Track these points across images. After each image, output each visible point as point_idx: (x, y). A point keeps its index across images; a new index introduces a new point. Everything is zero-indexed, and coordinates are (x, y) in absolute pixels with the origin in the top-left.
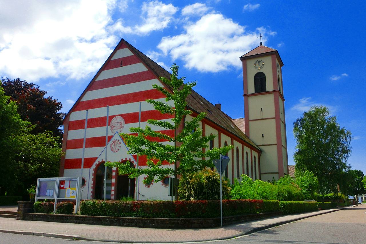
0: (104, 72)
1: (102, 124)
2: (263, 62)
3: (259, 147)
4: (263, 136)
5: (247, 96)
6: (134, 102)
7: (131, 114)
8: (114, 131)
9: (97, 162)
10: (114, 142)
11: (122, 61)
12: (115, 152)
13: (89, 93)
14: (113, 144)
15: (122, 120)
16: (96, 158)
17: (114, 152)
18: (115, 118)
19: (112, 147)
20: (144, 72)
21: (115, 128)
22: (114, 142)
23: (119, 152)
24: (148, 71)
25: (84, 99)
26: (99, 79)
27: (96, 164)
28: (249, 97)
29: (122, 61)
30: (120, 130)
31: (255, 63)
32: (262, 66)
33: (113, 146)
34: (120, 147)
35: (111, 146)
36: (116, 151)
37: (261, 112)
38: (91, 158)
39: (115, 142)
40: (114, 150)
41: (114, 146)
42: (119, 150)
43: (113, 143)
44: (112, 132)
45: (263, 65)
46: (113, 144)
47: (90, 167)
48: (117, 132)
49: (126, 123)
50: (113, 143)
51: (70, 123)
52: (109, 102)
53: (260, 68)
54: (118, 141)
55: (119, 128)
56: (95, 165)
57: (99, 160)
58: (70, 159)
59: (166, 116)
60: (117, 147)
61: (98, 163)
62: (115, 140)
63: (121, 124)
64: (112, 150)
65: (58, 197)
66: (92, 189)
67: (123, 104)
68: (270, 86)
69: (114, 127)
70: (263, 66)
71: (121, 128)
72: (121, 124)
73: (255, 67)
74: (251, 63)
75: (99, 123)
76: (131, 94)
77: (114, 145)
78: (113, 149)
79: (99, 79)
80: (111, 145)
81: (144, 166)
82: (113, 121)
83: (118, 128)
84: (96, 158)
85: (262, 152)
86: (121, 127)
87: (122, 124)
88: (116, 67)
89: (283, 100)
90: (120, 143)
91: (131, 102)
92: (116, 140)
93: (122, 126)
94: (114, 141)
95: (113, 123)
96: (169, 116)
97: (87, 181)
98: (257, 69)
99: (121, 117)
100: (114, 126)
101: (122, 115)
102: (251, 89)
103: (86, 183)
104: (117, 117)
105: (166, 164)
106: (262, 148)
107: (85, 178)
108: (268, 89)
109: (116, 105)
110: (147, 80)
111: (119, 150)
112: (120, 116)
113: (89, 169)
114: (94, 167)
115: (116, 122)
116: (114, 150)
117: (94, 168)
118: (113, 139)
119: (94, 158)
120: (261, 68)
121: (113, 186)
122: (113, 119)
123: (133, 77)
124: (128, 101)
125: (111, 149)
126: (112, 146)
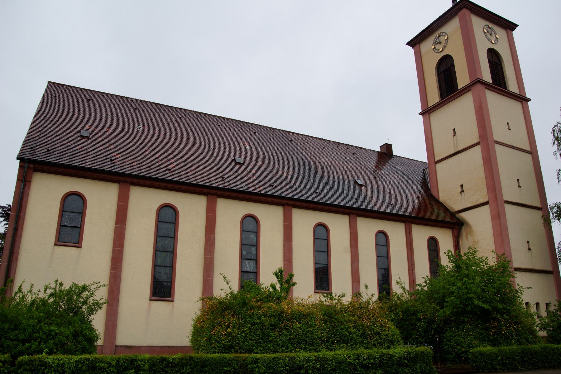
2: (446, 34)
3: (457, 215)
4: (463, 191)
5: (427, 112)
28: (431, 115)
31: (433, 43)
32: (446, 42)
53: (441, 50)
68: (462, 80)
70: (447, 42)
74: (427, 46)
85: (463, 227)
89: (523, 99)
98: (438, 53)
102: (434, 97)
106: (464, 215)
120: (444, 47)
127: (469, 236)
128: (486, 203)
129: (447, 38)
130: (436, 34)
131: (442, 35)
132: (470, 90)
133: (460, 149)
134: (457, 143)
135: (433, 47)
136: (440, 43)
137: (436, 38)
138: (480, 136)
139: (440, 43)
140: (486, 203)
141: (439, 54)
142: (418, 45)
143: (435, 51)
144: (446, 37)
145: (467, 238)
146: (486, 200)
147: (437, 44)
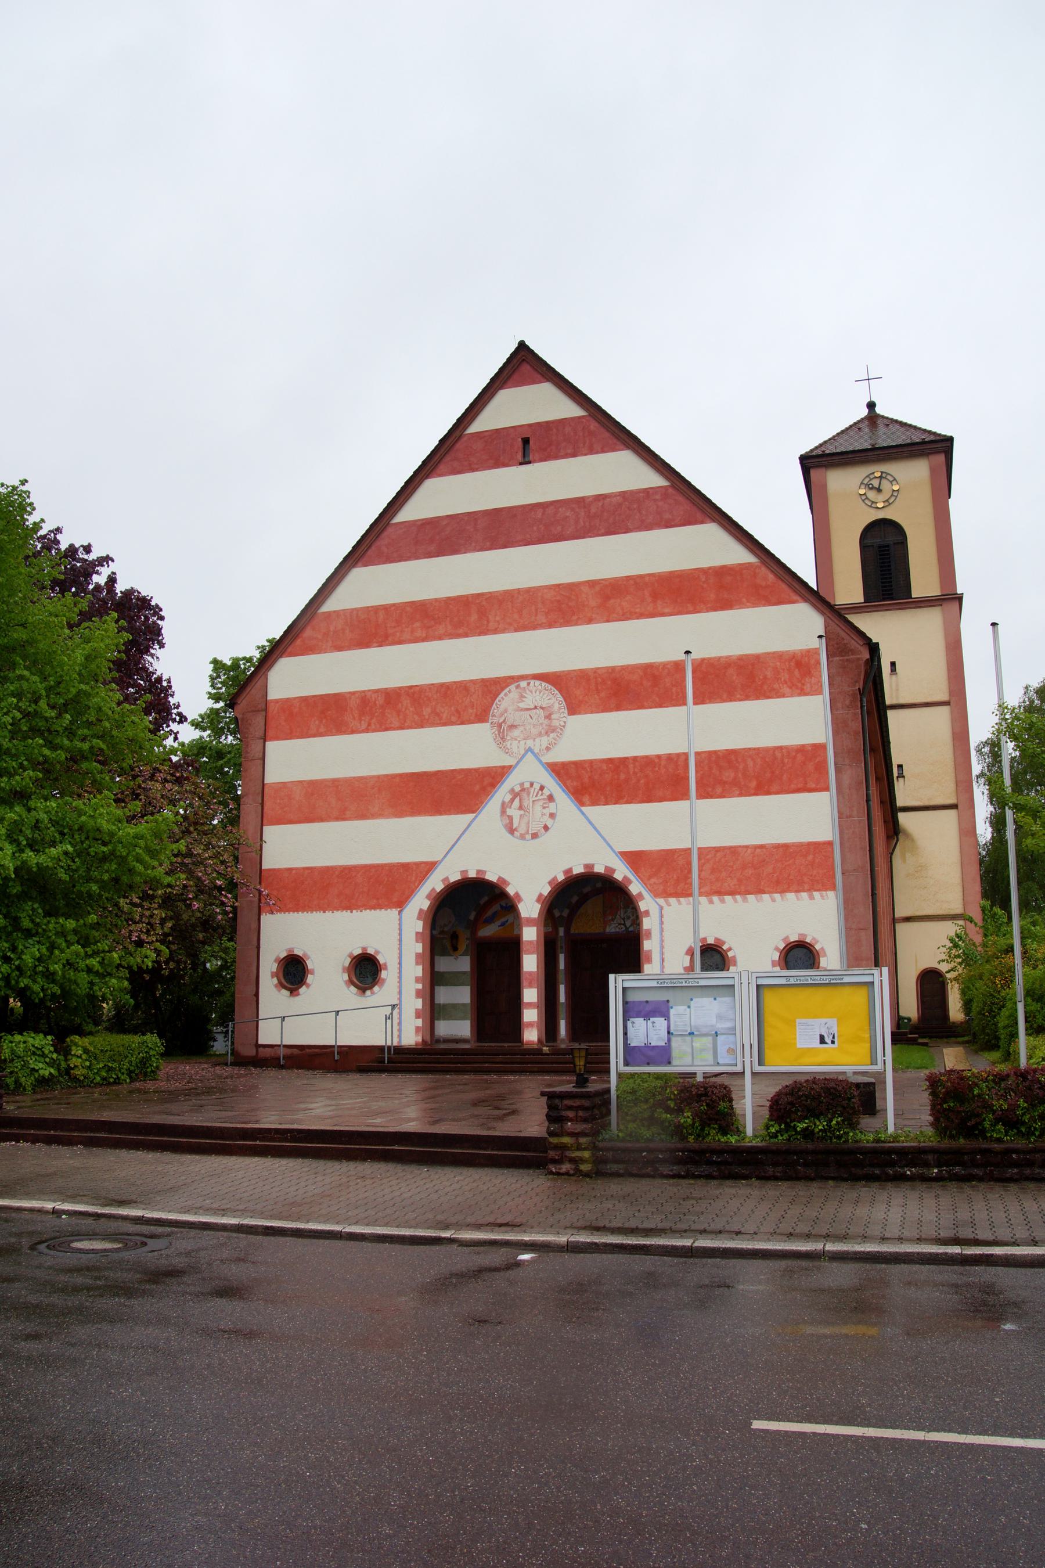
0: (431, 486)
1: (444, 716)
2: (895, 479)
6: (608, 621)
7: (595, 671)
8: (517, 747)
9: (435, 883)
10: (515, 795)
11: (526, 441)
12: (529, 837)
13: (358, 574)
14: (516, 803)
15: (554, 700)
16: (430, 867)
17: (522, 837)
18: (513, 687)
19: (511, 818)
20: (647, 493)
21: (516, 733)
22: (515, 795)
23: (545, 838)
24: (671, 490)
25: (337, 602)
26: (408, 514)
27: (433, 890)
29: (526, 441)
30: (545, 741)
31: (862, 483)
32: (892, 495)
33: (513, 812)
34: (552, 816)
35: (503, 812)
36: (535, 836)
37: (894, 677)
38: (406, 867)
39: (524, 795)
40: (522, 830)
41: (522, 812)
42: (546, 828)
43: (512, 800)
44: (507, 752)
45: (895, 494)
46: (516, 803)
47: (400, 904)
48: (530, 750)
49: (573, 711)
50: (512, 800)
51: (272, 708)
52: (474, 617)
54: (542, 788)
55: (540, 735)
56: (428, 897)
57: (450, 872)
58: (290, 870)
59: (776, 686)
60: (538, 814)
61: (440, 887)
62: (522, 784)
63: (548, 717)
64: (511, 830)
65: (761, 1063)
66: (420, 1001)
67: (550, 625)
69: (513, 727)
70: (896, 497)
71: (552, 735)
72: (548, 717)
73: (864, 498)
75: (429, 710)
76: (592, 584)
77: (521, 808)
78: (515, 826)
79: (411, 512)
80: (504, 807)
81: (682, 899)
82: (507, 701)
83: (535, 731)
84: (430, 867)
86: (551, 730)
87: (554, 716)
88: (498, 463)
90: (551, 798)
91: (590, 621)
92: (527, 785)
93: (555, 723)
94: (517, 789)
95: (506, 711)
96: (790, 688)
97: (389, 967)
98: (871, 506)
99: (544, 684)
100: (509, 723)
101: (554, 680)
103: (384, 974)
104: (523, 684)
105: (791, 892)
107: (377, 952)
108: (918, 590)
109: (516, 630)
110: (668, 525)
111: (546, 828)
112: (537, 683)
113: (395, 912)
114: (421, 901)
115: (522, 705)
116: (522, 830)
117: (421, 910)
118: (511, 782)
119: (418, 864)
120: (888, 503)
121: (530, 986)
122: (502, 695)
123: (593, 510)
124: (575, 618)
125: (505, 826)
126: (509, 812)
127: (908, 855)
128: (954, 806)
129: (898, 490)
130: (877, 469)
131: (885, 478)
132: (941, 605)
133: (902, 701)
134: (897, 690)
135: (862, 491)
136: (879, 490)
137: (868, 476)
138: (951, 693)
139: (879, 490)
140: (954, 806)
141: (873, 511)
142: (823, 470)
143: (863, 501)
144: (896, 488)
145: (904, 860)
146: (952, 801)
147: (871, 489)
